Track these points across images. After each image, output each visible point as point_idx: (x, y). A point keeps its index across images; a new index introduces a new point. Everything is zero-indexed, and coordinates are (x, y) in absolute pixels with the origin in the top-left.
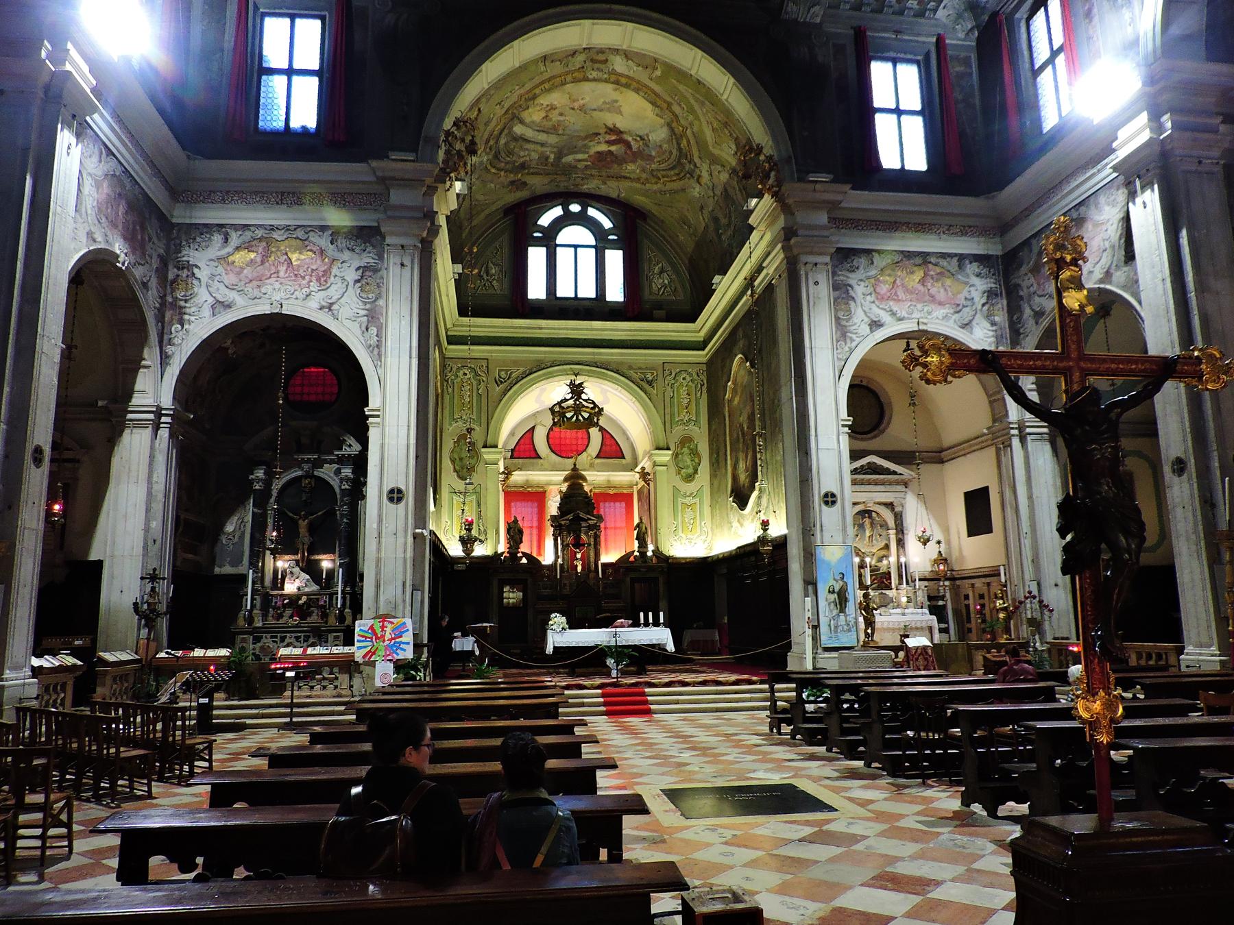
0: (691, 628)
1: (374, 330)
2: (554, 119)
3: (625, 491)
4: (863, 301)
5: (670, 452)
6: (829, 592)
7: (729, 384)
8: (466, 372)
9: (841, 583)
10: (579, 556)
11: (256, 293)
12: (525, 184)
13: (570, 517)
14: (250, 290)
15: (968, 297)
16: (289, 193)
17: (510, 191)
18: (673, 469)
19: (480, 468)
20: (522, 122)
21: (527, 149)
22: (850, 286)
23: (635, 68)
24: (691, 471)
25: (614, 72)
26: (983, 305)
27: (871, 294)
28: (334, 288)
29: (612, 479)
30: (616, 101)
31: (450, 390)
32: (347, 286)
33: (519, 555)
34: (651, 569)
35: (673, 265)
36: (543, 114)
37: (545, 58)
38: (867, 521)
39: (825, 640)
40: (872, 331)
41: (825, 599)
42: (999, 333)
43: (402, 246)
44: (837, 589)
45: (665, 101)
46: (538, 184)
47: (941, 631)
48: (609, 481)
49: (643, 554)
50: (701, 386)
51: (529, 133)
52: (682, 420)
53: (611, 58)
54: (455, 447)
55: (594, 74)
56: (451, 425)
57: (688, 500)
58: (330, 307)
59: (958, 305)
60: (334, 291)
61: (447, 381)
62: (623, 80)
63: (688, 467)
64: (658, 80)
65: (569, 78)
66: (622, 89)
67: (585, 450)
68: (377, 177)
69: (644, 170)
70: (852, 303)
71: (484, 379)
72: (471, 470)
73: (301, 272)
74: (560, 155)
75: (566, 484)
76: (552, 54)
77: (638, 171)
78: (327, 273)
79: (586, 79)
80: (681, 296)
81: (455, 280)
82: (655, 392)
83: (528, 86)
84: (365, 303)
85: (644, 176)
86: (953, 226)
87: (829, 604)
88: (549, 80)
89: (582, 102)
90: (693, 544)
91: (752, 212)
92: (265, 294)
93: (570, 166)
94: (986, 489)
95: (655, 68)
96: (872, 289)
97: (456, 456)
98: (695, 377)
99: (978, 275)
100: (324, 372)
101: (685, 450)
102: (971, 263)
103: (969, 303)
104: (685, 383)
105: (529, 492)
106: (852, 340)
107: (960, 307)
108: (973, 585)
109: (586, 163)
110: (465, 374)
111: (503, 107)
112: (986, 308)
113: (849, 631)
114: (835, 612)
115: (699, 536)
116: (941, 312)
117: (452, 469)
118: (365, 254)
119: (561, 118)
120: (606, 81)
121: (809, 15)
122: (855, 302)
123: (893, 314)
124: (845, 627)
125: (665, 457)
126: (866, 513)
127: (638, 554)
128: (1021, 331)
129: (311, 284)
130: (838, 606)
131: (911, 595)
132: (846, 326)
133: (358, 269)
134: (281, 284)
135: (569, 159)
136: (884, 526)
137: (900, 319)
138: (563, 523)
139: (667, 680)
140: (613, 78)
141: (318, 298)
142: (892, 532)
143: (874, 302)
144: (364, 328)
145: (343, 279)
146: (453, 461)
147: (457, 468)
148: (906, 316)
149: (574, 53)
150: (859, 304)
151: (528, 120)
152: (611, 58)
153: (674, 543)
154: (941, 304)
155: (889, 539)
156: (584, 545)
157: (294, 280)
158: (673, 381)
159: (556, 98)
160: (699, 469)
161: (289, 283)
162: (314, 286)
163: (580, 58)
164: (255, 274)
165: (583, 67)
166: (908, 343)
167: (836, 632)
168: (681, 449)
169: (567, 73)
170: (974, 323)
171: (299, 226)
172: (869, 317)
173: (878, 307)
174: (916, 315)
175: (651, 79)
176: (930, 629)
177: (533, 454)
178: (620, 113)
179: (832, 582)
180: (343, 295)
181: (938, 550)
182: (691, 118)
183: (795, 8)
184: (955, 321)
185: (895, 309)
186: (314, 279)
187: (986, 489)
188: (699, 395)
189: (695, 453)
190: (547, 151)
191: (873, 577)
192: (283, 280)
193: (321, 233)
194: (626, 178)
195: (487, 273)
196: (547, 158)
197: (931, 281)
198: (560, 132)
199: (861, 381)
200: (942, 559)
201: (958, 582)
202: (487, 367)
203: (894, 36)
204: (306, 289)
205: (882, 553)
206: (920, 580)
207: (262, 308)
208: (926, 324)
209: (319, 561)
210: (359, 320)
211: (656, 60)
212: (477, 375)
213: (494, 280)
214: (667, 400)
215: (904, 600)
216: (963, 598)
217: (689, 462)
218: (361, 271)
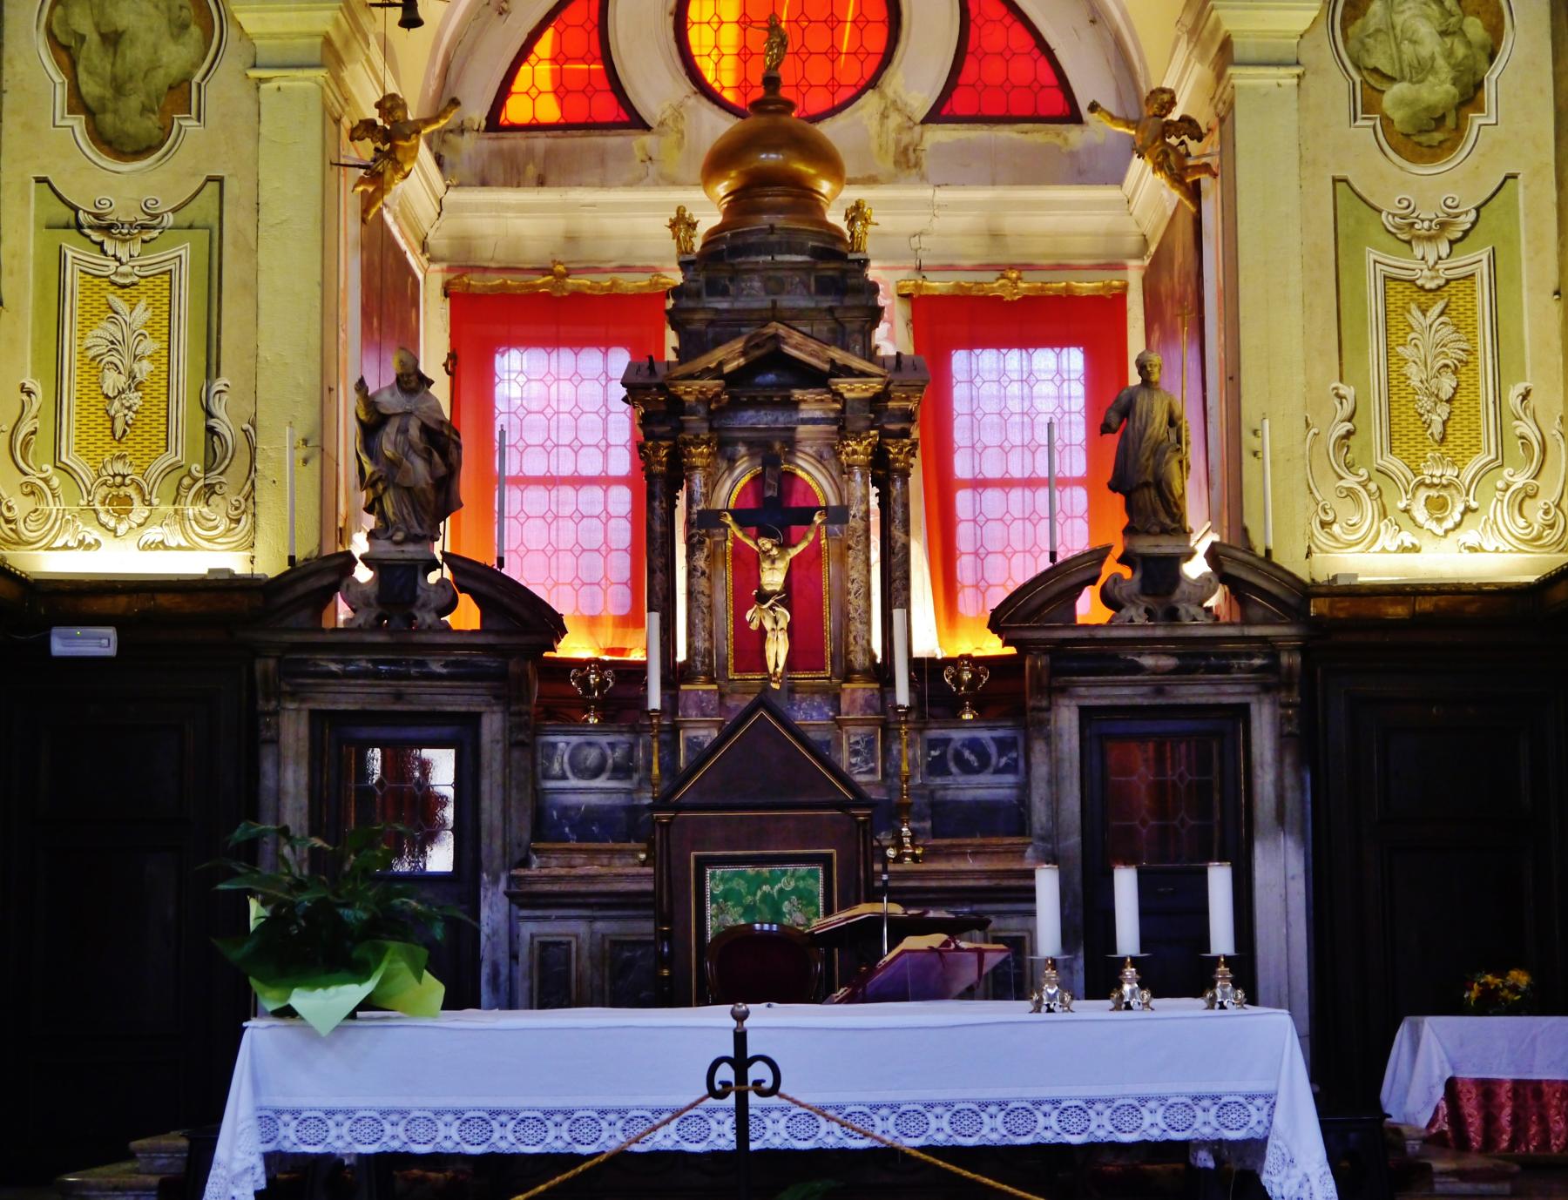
0: (1456, 1007)
3: (1086, 285)
10: (773, 578)
13: (730, 356)
24: (1439, 90)
29: (1011, 222)
48: (995, 236)
63: (1422, 70)
67: (873, 82)
75: (722, 188)
105: (578, 296)
115: (1485, 471)
117: (61, 94)
138: (689, 391)
146: (66, 51)
147: (90, 88)
153: (1344, 508)
156: (805, 516)
160: (1492, 77)
177: (605, 107)
217: (1428, 40)
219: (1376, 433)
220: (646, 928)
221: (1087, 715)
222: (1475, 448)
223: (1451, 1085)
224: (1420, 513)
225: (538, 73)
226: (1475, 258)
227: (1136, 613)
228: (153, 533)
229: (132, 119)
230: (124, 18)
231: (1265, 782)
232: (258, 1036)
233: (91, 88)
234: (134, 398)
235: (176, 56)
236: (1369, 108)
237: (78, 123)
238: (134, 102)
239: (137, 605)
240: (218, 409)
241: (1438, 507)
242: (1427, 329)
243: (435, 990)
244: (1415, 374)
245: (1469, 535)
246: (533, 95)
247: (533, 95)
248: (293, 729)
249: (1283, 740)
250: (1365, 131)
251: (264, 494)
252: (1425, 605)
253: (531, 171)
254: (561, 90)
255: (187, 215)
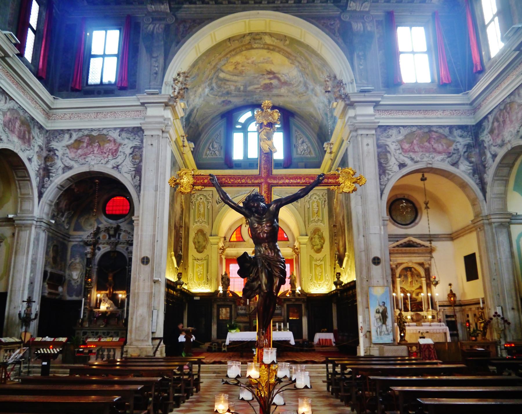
0: (320, 332)
1: (138, 178)
2: (240, 69)
3: (289, 258)
4: (395, 153)
5: (308, 237)
6: (377, 312)
7: (335, 200)
8: (202, 197)
9: (383, 307)
11: (83, 161)
12: (230, 102)
14: (81, 160)
15: (455, 148)
16: (100, 113)
17: (223, 106)
18: (310, 246)
19: (208, 247)
20: (223, 71)
21: (227, 85)
22: (387, 145)
23: (276, 41)
24: (319, 247)
25: (266, 44)
26: (465, 152)
27: (399, 149)
28: (119, 157)
30: (269, 58)
31: (193, 207)
32: (126, 156)
33: (228, 292)
34: (297, 300)
35: (308, 138)
36: (233, 67)
37: (229, 39)
38: (409, 273)
39: (374, 339)
40: (400, 169)
41: (374, 317)
42: (475, 167)
43: (152, 136)
44: (381, 311)
45: (293, 56)
46: (237, 101)
47: (451, 335)
49: (294, 292)
50: (325, 201)
51: (228, 77)
52: (314, 220)
53: (263, 36)
54: (195, 236)
55: (256, 46)
56: (194, 225)
57: (318, 263)
58: (117, 167)
59: (450, 153)
60: (120, 160)
61: (192, 202)
62: (271, 47)
63: (318, 245)
64: (288, 46)
65: (244, 48)
66: (271, 52)
68: (141, 103)
69: (289, 91)
70: (388, 155)
71: (211, 201)
72: (204, 247)
73: (105, 151)
74: (245, 86)
76: (233, 37)
77: (286, 92)
78: (116, 151)
79: (252, 48)
80: (313, 155)
81: (192, 152)
82: (300, 205)
83: (223, 54)
84: (134, 165)
85: (290, 94)
86: (446, 111)
87: (377, 319)
88: (234, 50)
89: (252, 60)
90: (321, 286)
91: (334, 109)
92: (87, 162)
93: (252, 92)
94: (474, 254)
95: (286, 40)
96: (400, 147)
97: (196, 241)
98: (321, 197)
99: (461, 136)
100: (123, 199)
101: (316, 236)
102: (456, 130)
103: (456, 152)
104: (316, 200)
106: (389, 174)
107: (451, 154)
108: (470, 309)
109: (260, 89)
110: (201, 199)
111: (211, 65)
112: (466, 154)
113: (388, 334)
114: (380, 324)
115: (324, 282)
116: (440, 157)
118: (134, 141)
119: (243, 68)
120: (263, 48)
121: (362, 8)
122: (390, 154)
123: (412, 159)
124: (386, 332)
125: (305, 239)
126: (408, 269)
127: (291, 292)
128: (486, 166)
129: (109, 156)
130: (382, 321)
131: (435, 314)
132: (385, 167)
133: (131, 148)
134: (95, 156)
135: (250, 88)
136: (419, 275)
137: (416, 162)
139: (304, 360)
140: (266, 47)
141: (112, 163)
142: (424, 280)
143: (401, 153)
144: (133, 177)
145: (124, 153)
146: (195, 243)
148: (420, 160)
149: (244, 36)
150: (392, 154)
151: (226, 70)
152: (263, 36)
154: (440, 153)
155: (421, 283)
157: (101, 155)
158: (309, 200)
159: (238, 58)
160: (324, 246)
161: (99, 156)
162: (110, 157)
163: (248, 38)
164: (83, 152)
165: (250, 42)
166: (423, 175)
167: (381, 334)
168: (314, 235)
169: (243, 46)
170: (460, 162)
171: (104, 129)
172: (398, 161)
173: (404, 156)
174: (425, 159)
175: (285, 46)
176: (445, 334)
177: (241, 240)
178: (272, 63)
179: (378, 307)
180: (124, 161)
181: (450, 289)
182: (307, 63)
183: (354, 4)
184: (448, 162)
185: (413, 156)
186: (110, 154)
187: (474, 254)
188: (323, 206)
189: (321, 238)
190: (239, 84)
191: (413, 305)
192: (96, 155)
193: (114, 131)
194: (281, 96)
195: (213, 147)
196: (239, 89)
197: (434, 140)
198: (244, 75)
199: (404, 196)
200: (452, 294)
201: (463, 307)
202: (212, 195)
203: (410, 14)
204: (107, 159)
205: (418, 291)
206: (439, 306)
207: (85, 169)
208: (430, 164)
209: (117, 295)
210: (131, 173)
211: (285, 36)
212: (207, 199)
213: (216, 150)
214: (306, 210)
215: (430, 317)
216: (466, 316)
218: (132, 149)
219: (314, 279)
220: (248, 325)
221: (287, 305)
222: (323, 280)
223: (319, 339)
224: (318, 286)
225: (234, 236)
226: (323, 263)
227: (292, 296)
228: (202, 288)
229: (201, 250)
230: (200, 240)
231: (303, 311)
232: (229, 333)
233: (197, 247)
234: (201, 275)
235: (204, 244)
236: (313, 248)
237: (195, 250)
238: (201, 248)
239: (202, 295)
240: (208, 276)
241: (319, 285)
242: (318, 268)
243: (239, 330)
244: (317, 273)
245: (322, 288)
246: (234, 238)
247: (234, 238)
248: (215, 306)
249: (305, 307)
250: (312, 251)
251: (212, 284)
252: (317, 295)
253: (234, 246)
254: (236, 238)
255: (206, 258)
